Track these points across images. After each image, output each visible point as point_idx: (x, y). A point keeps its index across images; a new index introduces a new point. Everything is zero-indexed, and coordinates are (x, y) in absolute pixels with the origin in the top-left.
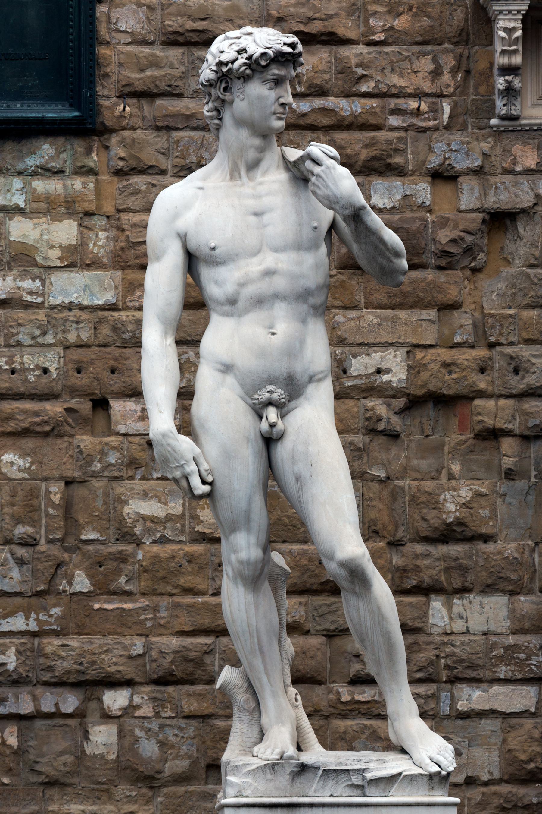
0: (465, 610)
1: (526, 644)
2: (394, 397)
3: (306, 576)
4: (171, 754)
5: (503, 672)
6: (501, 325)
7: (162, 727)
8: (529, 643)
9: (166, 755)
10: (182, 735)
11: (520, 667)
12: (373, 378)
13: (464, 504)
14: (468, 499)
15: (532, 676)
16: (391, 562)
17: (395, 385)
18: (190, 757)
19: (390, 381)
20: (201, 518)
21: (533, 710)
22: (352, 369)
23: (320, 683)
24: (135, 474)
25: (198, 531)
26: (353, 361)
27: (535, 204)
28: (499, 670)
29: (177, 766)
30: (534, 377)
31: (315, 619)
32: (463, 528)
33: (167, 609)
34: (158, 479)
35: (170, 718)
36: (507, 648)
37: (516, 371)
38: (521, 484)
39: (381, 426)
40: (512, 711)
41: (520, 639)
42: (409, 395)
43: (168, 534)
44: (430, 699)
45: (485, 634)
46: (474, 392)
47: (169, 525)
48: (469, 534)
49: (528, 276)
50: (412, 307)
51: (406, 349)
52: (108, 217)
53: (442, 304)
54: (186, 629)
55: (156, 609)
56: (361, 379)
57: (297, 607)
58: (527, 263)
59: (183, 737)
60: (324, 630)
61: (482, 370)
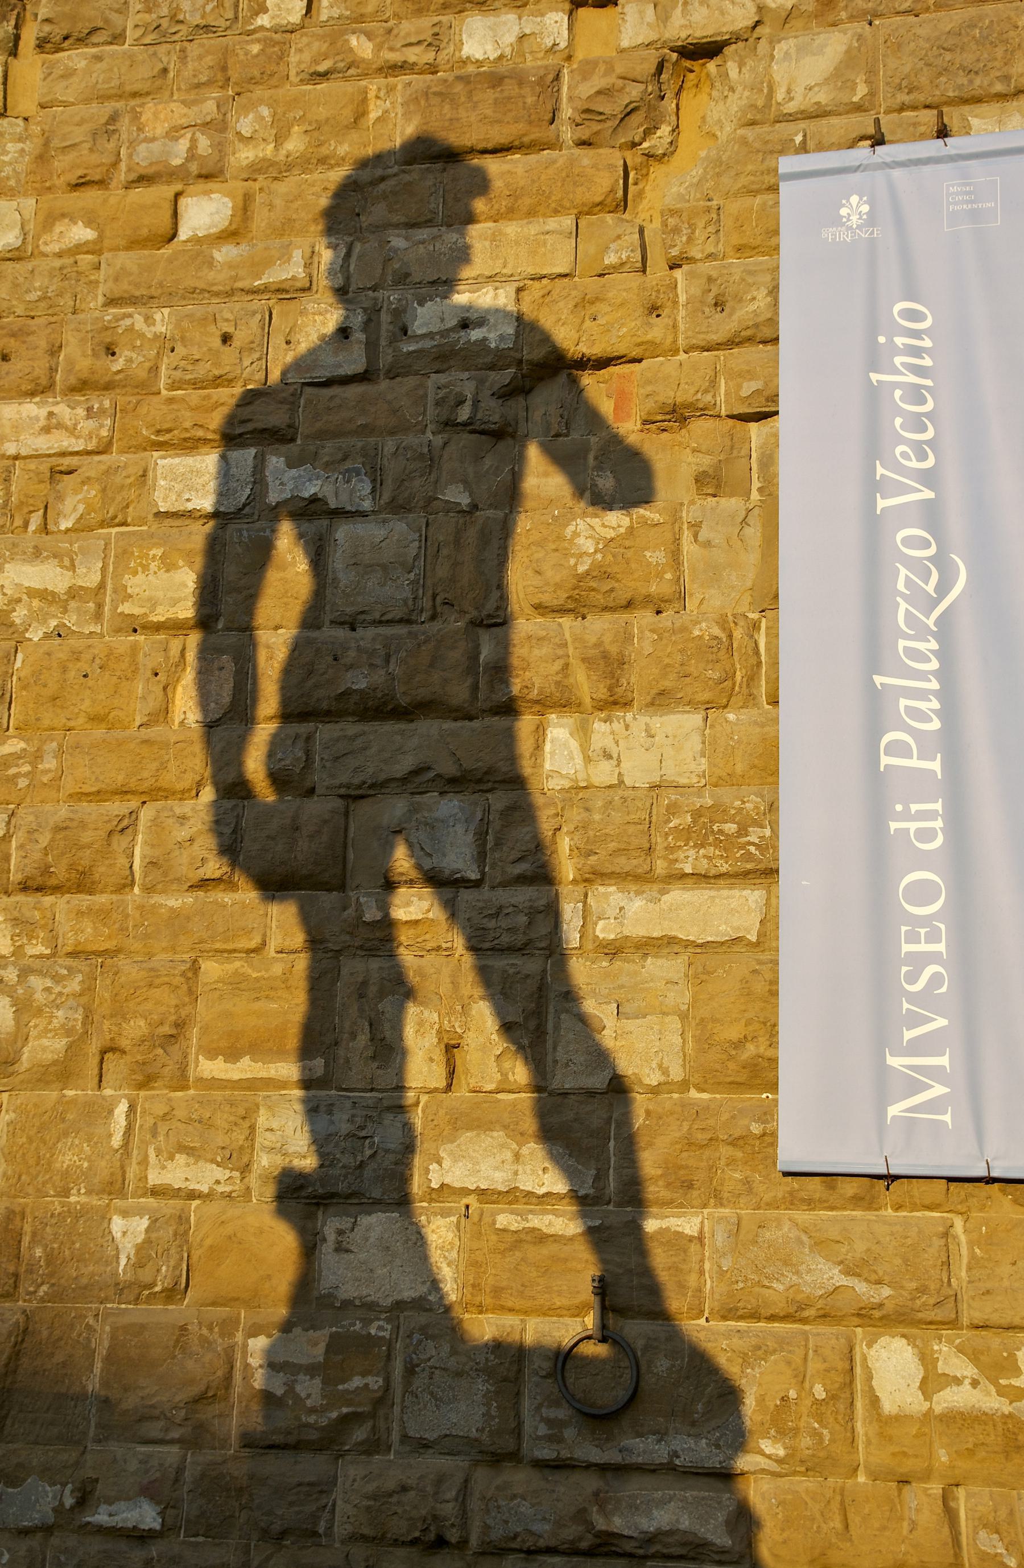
0: (617, 743)
1: (738, 803)
2: (492, 367)
3: (310, 683)
4: (36, 1026)
5: (689, 861)
6: (690, 226)
7: (24, 973)
8: (744, 803)
9: (26, 1030)
10: (57, 989)
11: (725, 850)
13: (612, 540)
16: (474, 656)
17: (493, 345)
18: (69, 1032)
19: (485, 339)
20: (129, 590)
21: (753, 938)
25: (122, 613)
26: (419, 310)
27: (758, 23)
28: (682, 856)
29: (44, 1049)
30: (752, 307)
31: (324, 767)
33: (60, 752)
35: (41, 956)
36: (697, 814)
37: (719, 304)
38: (731, 504)
39: (464, 414)
40: (709, 939)
41: (727, 795)
42: (520, 362)
43: (70, 621)
44: (541, 916)
45: (653, 787)
46: (639, 345)
47: (73, 604)
48: (623, 596)
49: (744, 141)
50: (531, 213)
51: (516, 285)
52: (26, 119)
53: (583, 204)
54: (87, 789)
55: (38, 757)
56: (432, 339)
57: (289, 742)
58: (744, 121)
59: (60, 994)
61: (654, 309)
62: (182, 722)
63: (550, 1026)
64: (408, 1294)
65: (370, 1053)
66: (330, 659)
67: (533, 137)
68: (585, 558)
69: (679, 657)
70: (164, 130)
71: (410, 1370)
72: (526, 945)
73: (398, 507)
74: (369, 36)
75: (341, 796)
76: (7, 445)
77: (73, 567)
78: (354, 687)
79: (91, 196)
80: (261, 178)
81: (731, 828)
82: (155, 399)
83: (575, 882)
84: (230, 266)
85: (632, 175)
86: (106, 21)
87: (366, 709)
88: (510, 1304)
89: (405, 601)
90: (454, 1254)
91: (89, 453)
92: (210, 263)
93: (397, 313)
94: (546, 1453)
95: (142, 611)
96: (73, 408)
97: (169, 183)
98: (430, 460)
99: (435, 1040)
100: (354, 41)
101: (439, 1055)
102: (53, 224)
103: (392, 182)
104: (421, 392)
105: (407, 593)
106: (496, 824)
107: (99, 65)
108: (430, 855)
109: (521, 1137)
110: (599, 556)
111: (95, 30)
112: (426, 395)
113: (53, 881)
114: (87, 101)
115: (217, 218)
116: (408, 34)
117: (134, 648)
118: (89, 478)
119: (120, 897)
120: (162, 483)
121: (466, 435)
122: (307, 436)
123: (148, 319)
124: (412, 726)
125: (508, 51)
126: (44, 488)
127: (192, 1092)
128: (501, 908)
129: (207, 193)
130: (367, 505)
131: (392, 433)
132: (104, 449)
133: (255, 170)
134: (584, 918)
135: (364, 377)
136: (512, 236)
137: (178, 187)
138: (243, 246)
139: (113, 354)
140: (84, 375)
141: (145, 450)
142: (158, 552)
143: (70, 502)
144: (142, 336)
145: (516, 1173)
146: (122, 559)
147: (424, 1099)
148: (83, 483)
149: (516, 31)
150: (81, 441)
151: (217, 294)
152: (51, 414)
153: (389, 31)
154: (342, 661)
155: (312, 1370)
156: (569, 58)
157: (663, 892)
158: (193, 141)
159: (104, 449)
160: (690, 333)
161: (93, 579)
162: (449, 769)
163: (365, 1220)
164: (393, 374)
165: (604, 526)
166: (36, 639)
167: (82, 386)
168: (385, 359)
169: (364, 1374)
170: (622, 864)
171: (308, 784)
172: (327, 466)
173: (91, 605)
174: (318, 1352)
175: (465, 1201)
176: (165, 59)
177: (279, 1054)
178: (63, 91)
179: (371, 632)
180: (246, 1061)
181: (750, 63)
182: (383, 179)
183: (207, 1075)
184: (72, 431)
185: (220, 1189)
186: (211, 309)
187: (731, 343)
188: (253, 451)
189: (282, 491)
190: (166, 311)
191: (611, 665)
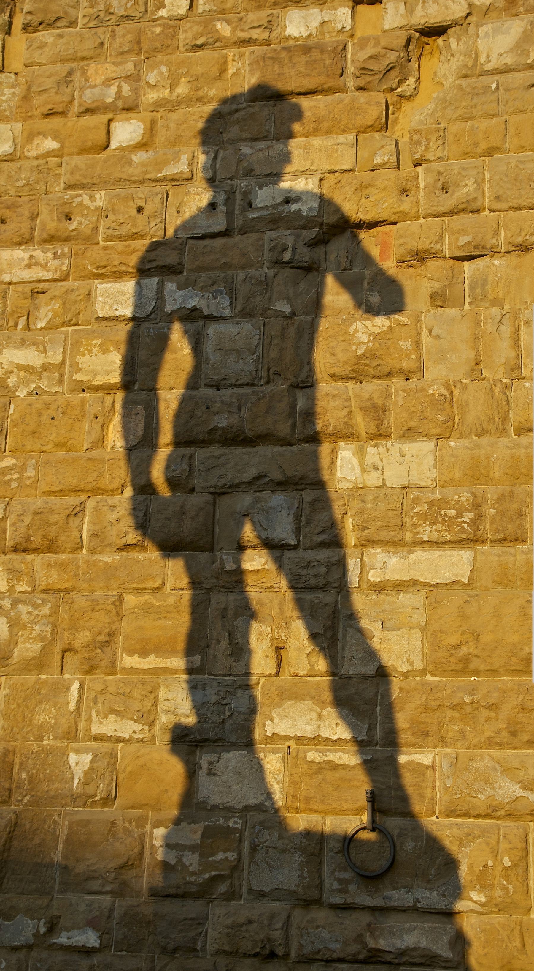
0: (382, 460)
2: (304, 227)
3: (192, 423)
5: (427, 533)
7: (15, 603)
8: (460, 497)
11: (449, 526)
12: (281, 208)
13: (378, 334)
14: (385, 328)
15: (463, 536)
16: (293, 406)
17: (305, 214)
18: (43, 639)
19: (300, 210)
20: (80, 366)
22: (257, 200)
23: (203, 550)
24: (16, 325)
25: (75, 380)
26: (259, 192)
28: (422, 530)
29: (27, 650)
31: (200, 475)
32: (378, 361)
33: (37, 466)
34: (42, 328)
35: (25, 592)
38: (451, 312)
39: (287, 256)
40: (439, 581)
42: (322, 224)
43: (44, 384)
44: (335, 567)
47: (45, 374)
48: (385, 369)
50: (329, 132)
51: (319, 176)
53: (361, 127)
54: (54, 488)
55: (23, 469)
56: (267, 210)
57: (179, 460)
60: (211, 487)
62: (113, 448)
63: (340, 635)
64: (252, 802)
65: (229, 652)
66: (204, 408)
67: (329, 85)
68: (362, 346)
69: (420, 407)
70: (102, 81)
71: (254, 849)
72: (325, 585)
73: (246, 314)
74: (228, 22)
75: (211, 493)
76: (4, 276)
77: (45, 351)
78: (219, 426)
79: (56, 122)
80: (161, 110)
81: (452, 513)
82: (96, 247)
83: (355, 546)
84: (143, 165)
85: (391, 108)
86: (66, 13)
87: (226, 439)
88: (315, 807)
89: (251, 372)
90: (281, 777)
91: (55, 280)
92: (130, 163)
93: (246, 194)
94: (338, 900)
95: (87, 378)
96: (45, 253)
97: (104, 113)
98: (266, 285)
99: (269, 644)
100: (219, 26)
101: (271, 653)
102: (32, 139)
103: (243, 113)
104: (260, 243)
105: (252, 367)
106: (307, 511)
107: (61, 40)
108: (266, 530)
109: (322, 704)
110: (370, 345)
111: (59, 18)
112: (263, 245)
113: (33, 546)
114: (54, 63)
115: (134, 135)
116: (252, 21)
117: (83, 402)
118: (55, 296)
119: (74, 555)
120: (100, 299)
121: (288, 270)
122: (190, 270)
123: (92, 198)
124: (255, 449)
125: (314, 32)
126: (27, 302)
127: (119, 676)
128: (310, 562)
129: (128, 119)
130: (227, 313)
131: (242, 268)
132: (64, 278)
133: (158, 105)
134: (361, 569)
135: (225, 234)
136: (317, 146)
137: (110, 116)
138: (150, 153)
139: (70, 219)
140: (52, 232)
141: (90, 278)
142: (98, 342)
143: (43, 311)
144: (88, 208)
145: (319, 727)
146: (75, 346)
147: (262, 680)
148: (51, 299)
149: (319, 20)
150: (50, 273)
151: (134, 182)
152: (31, 256)
153: (241, 19)
154: (212, 409)
155: (193, 848)
156: (352, 36)
157: (410, 552)
158: (120, 87)
159: (64, 278)
160: (426, 207)
161: (58, 359)
162: (278, 476)
163: (226, 756)
164: (243, 232)
165: (373, 325)
166: (22, 396)
167: (51, 239)
168: (238, 222)
169: (225, 851)
170: (385, 535)
171: (191, 486)
172: (202, 288)
173: (57, 375)
174: (197, 838)
175: (288, 744)
176: (102, 37)
177: (173, 653)
178: (38, 56)
179: (230, 391)
180: (152, 657)
181: (464, 39)
182: (237, 111)
183: (128, 666)
184: (44, 267)
185: (136, 736)
186: (130, 191)
187: (452, 212)
188: (156, 279)
189: (174, 304)
190: (103, 193)
191: (378, 411)
